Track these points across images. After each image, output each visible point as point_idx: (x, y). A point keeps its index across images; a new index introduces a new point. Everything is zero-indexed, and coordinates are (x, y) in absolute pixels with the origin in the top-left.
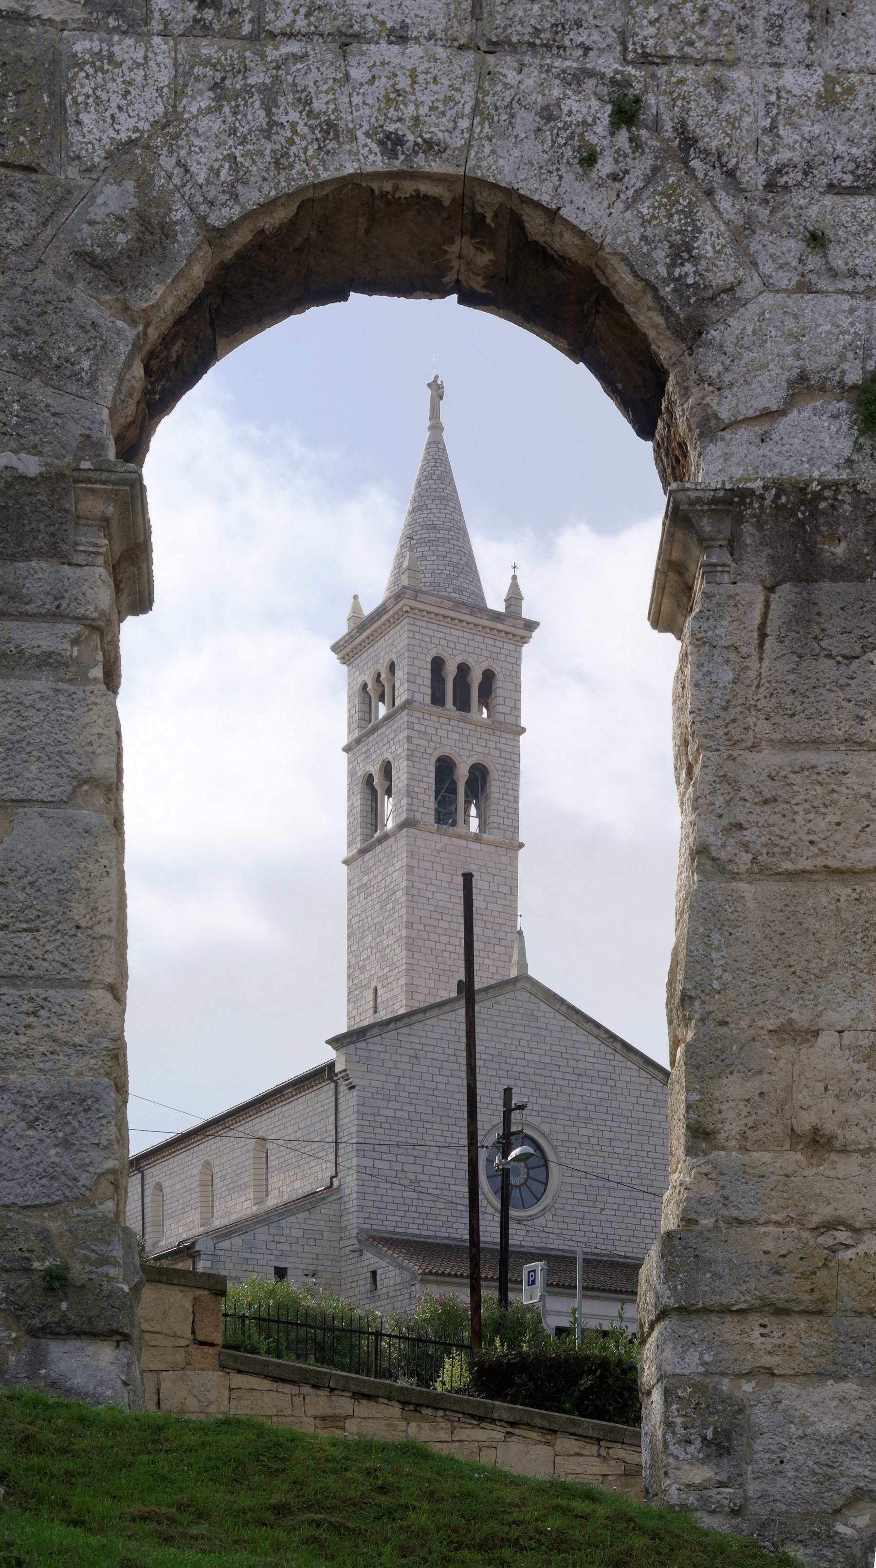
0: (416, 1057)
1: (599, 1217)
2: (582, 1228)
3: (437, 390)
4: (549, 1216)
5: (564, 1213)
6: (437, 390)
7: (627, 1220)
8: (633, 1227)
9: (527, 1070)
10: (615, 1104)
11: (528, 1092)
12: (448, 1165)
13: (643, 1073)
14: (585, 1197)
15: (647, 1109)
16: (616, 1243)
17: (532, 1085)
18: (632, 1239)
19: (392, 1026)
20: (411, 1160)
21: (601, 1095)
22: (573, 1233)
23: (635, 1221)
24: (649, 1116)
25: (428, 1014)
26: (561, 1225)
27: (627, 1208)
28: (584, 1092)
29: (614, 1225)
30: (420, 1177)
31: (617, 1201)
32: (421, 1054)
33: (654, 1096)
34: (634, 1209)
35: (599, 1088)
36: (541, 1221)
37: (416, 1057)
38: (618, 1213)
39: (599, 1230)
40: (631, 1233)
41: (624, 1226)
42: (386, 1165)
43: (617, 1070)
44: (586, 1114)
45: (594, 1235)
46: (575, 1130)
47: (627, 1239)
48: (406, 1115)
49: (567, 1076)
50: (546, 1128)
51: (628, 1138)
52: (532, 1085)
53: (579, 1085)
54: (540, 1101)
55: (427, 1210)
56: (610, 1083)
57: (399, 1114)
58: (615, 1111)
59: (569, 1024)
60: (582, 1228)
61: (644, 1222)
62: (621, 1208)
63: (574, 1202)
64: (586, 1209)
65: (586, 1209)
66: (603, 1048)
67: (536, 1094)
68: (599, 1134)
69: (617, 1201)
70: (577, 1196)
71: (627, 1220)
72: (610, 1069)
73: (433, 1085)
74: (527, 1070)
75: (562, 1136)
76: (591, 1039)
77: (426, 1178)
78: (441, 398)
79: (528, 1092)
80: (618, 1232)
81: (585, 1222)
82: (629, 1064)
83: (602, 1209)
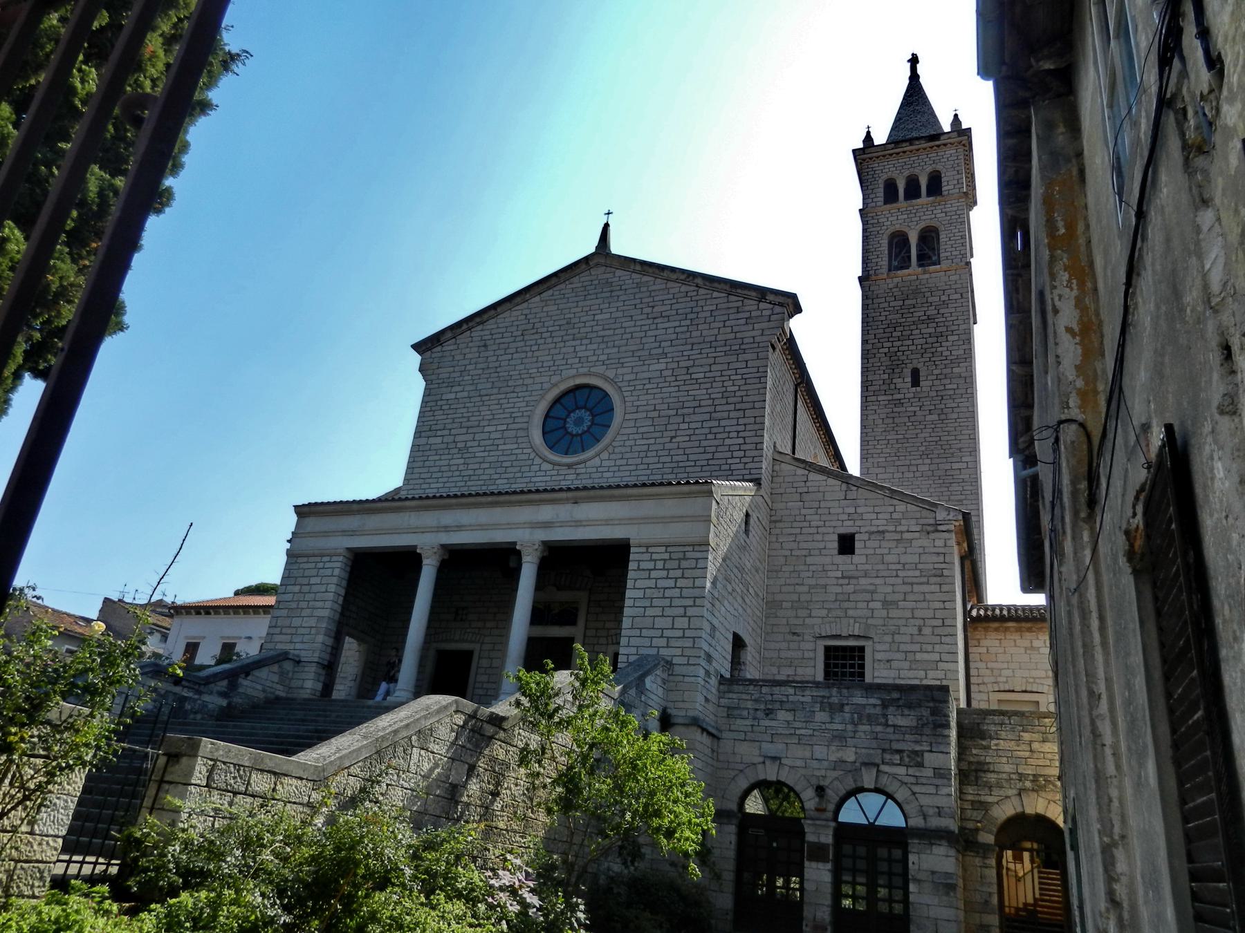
0: (485, 346)
1: (668, 446)
2: (645, 460)
3: (914, 61)
4: (605, 455)
5: (623, 450)
6: (914, 61)
7: (704, 443)
8: (713, 449)
9: (595, 328)
10: (694, 334)
11: (595, 346)
12: (499, 428)
13: (732, 298)
14: (652, 429)
15: (735, 329)
16: (688, 469)
17: (600, 340)
18: (711, 462)
19: (465, 327)
20: (464, 430)
21: (678, 330)
22: (633, 467)
23: (716, 442)
24: (738, 335)
25: (499, 310)
26: (618, 463)
27: (707, 431)
28: (657, 332)
29: (687, 451)
30: (469, 444)
31: (693, 425)
32: (488, 343)
33: (747, 315)
34: (714, 430)
35: (677, 324)
36: (597, 461)
37: (485, 346)
38: (693, 438)
39: (669, 459)
40: (710, 456)
41: (702, 450)
42: (439, 440)
43: (701, 303)
44: (660, 351)
45: (660, 466)
46: (645, 368)
47: (705, 463)
48: (465, 394)
49: (639, 323)
50: (611, 374)
51: (712, 361)
52: (600, 340)
53: (654, 327)
54: (607, 351)
55: (471, 472)
56: (689, 316)
57: (459, 395)
58: (695, 340)
59: (645, 279)
60: (645, 460)
61: (728, 442)
62: (697, 432)
63: (636, 436)
64: (652, 441)
65: (652, 441)
66: (684, 288)
67: (603, 346)
68: (675, 365)
69: (693, 425)
70: (641, 430)
71: (704, 443)
72: (693, 304)
73: (497, 364)
74: (595, 328)
75: (627, 378)
76: (670, 284)
77: (476, 443)
78: (918, 62)
79: (595, 346)
80: (691, 457)
81: (649, 454)
82: (715, 294)
83: (672, 438)
